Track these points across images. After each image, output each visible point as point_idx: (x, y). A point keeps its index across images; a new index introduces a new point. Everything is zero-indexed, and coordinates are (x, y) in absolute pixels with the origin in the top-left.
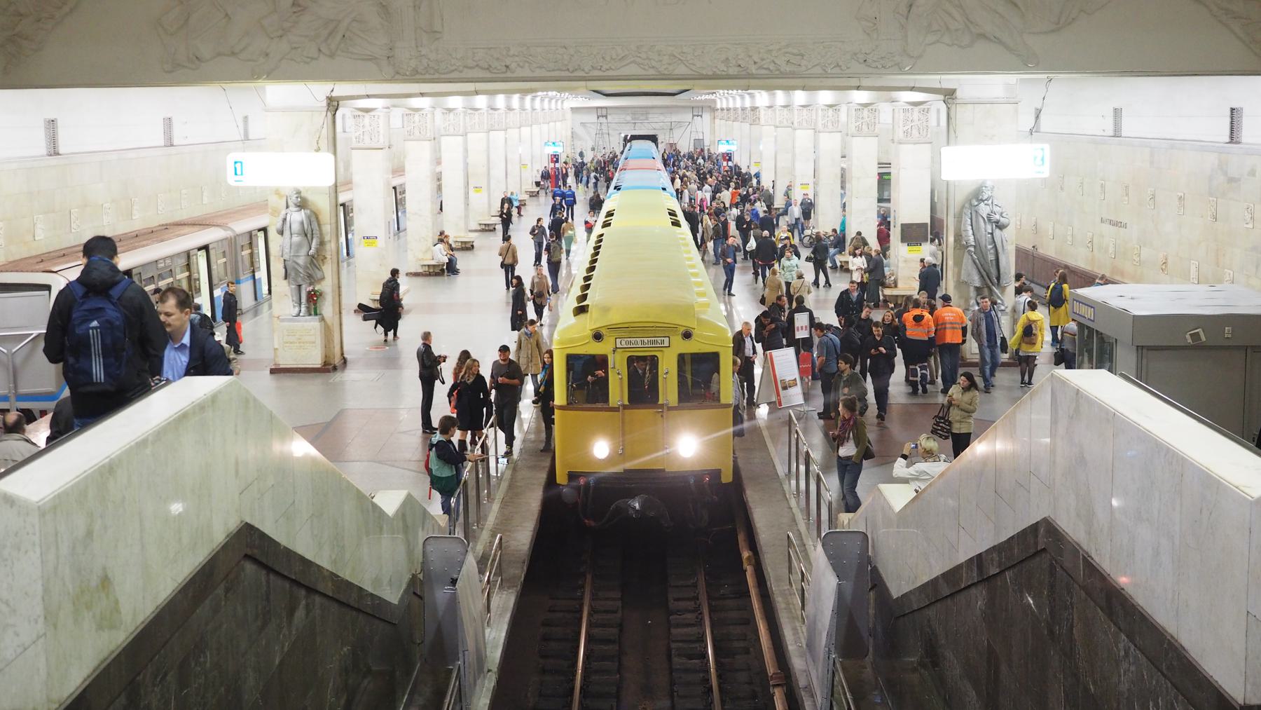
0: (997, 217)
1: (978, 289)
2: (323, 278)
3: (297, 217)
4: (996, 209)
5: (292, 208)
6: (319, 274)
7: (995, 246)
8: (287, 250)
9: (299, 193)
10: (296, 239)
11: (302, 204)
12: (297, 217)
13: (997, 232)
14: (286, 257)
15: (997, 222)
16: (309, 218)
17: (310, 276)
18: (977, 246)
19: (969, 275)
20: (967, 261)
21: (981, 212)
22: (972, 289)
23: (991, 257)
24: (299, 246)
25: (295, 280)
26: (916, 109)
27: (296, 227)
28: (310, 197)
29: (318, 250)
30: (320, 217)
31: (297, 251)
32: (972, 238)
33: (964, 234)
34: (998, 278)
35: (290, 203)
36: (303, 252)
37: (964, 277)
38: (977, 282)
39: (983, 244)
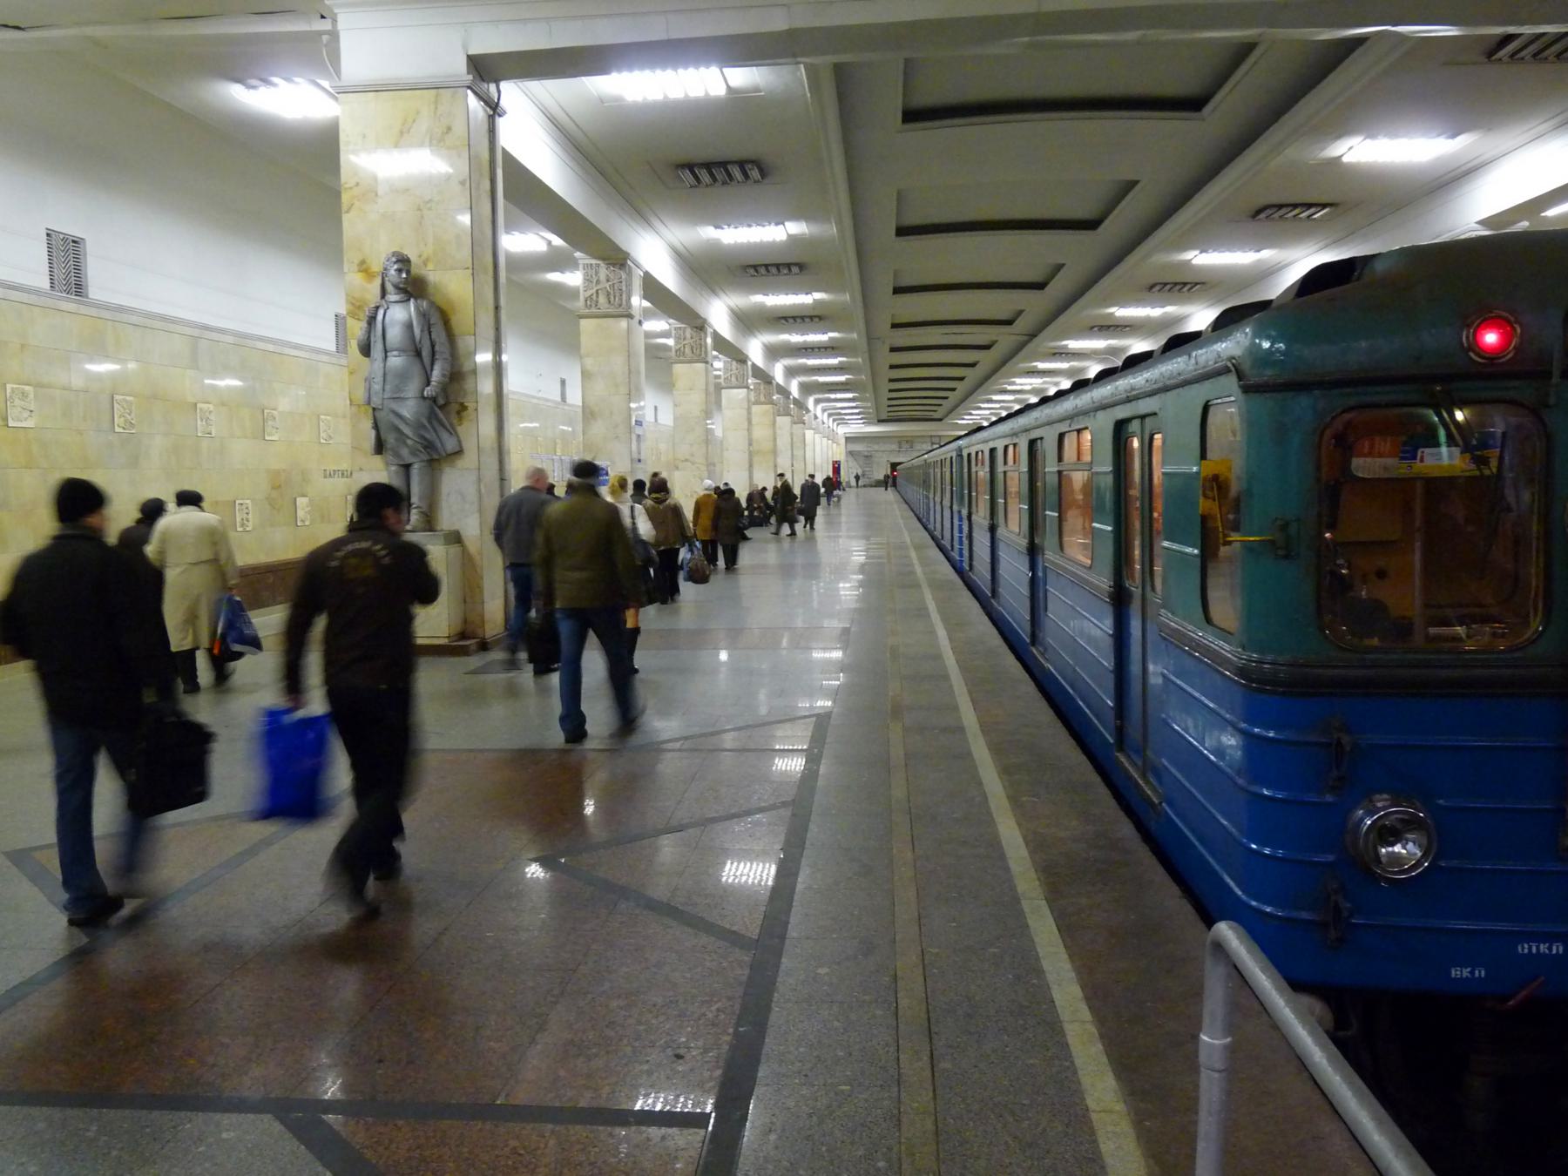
2: (459, 452)
3: (398, 315)
5: (393, 297)
6: (450, 444)
8: (377, 387)
9: (403, 261)
10: (396, 361)
11: (413, 288)
12: (398, 315)
14: (376, 401)
16: (423, 316)
17: (429, 446)
24: (403, 376)
25: (397, 455)
27: (395, 334)
28: (433, 276)
29: (445, 388)
30: (454, 321)
31: (398, 389)
35: (389, 287)
36: (412, 389)
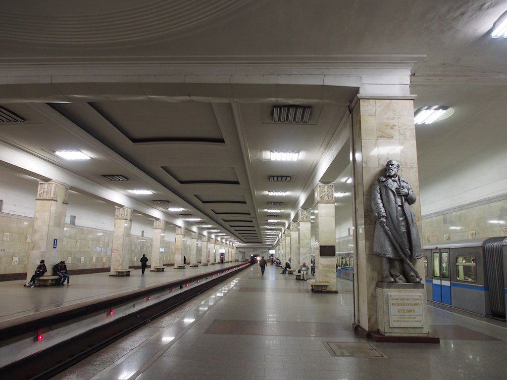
0: (406, 190)
1: (389, 259)
4: (402, 184)
7: (406, 219)
13: (406, 205)
15: (406, 195)
18: (389, 216)
19: (382, 246)
20: (379, 233)
21: (390, 186)
22: (385, 261)
23: (403, 229)
26: (326, 186)
32: (383, 210)
33: (374, 207)
34: (411, 249)
37: (377, 249)
38: (390, 254)
39: (394, 214)
